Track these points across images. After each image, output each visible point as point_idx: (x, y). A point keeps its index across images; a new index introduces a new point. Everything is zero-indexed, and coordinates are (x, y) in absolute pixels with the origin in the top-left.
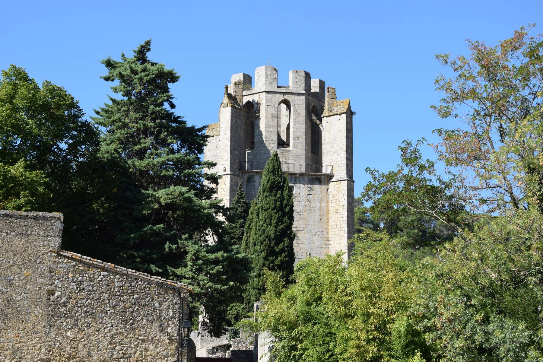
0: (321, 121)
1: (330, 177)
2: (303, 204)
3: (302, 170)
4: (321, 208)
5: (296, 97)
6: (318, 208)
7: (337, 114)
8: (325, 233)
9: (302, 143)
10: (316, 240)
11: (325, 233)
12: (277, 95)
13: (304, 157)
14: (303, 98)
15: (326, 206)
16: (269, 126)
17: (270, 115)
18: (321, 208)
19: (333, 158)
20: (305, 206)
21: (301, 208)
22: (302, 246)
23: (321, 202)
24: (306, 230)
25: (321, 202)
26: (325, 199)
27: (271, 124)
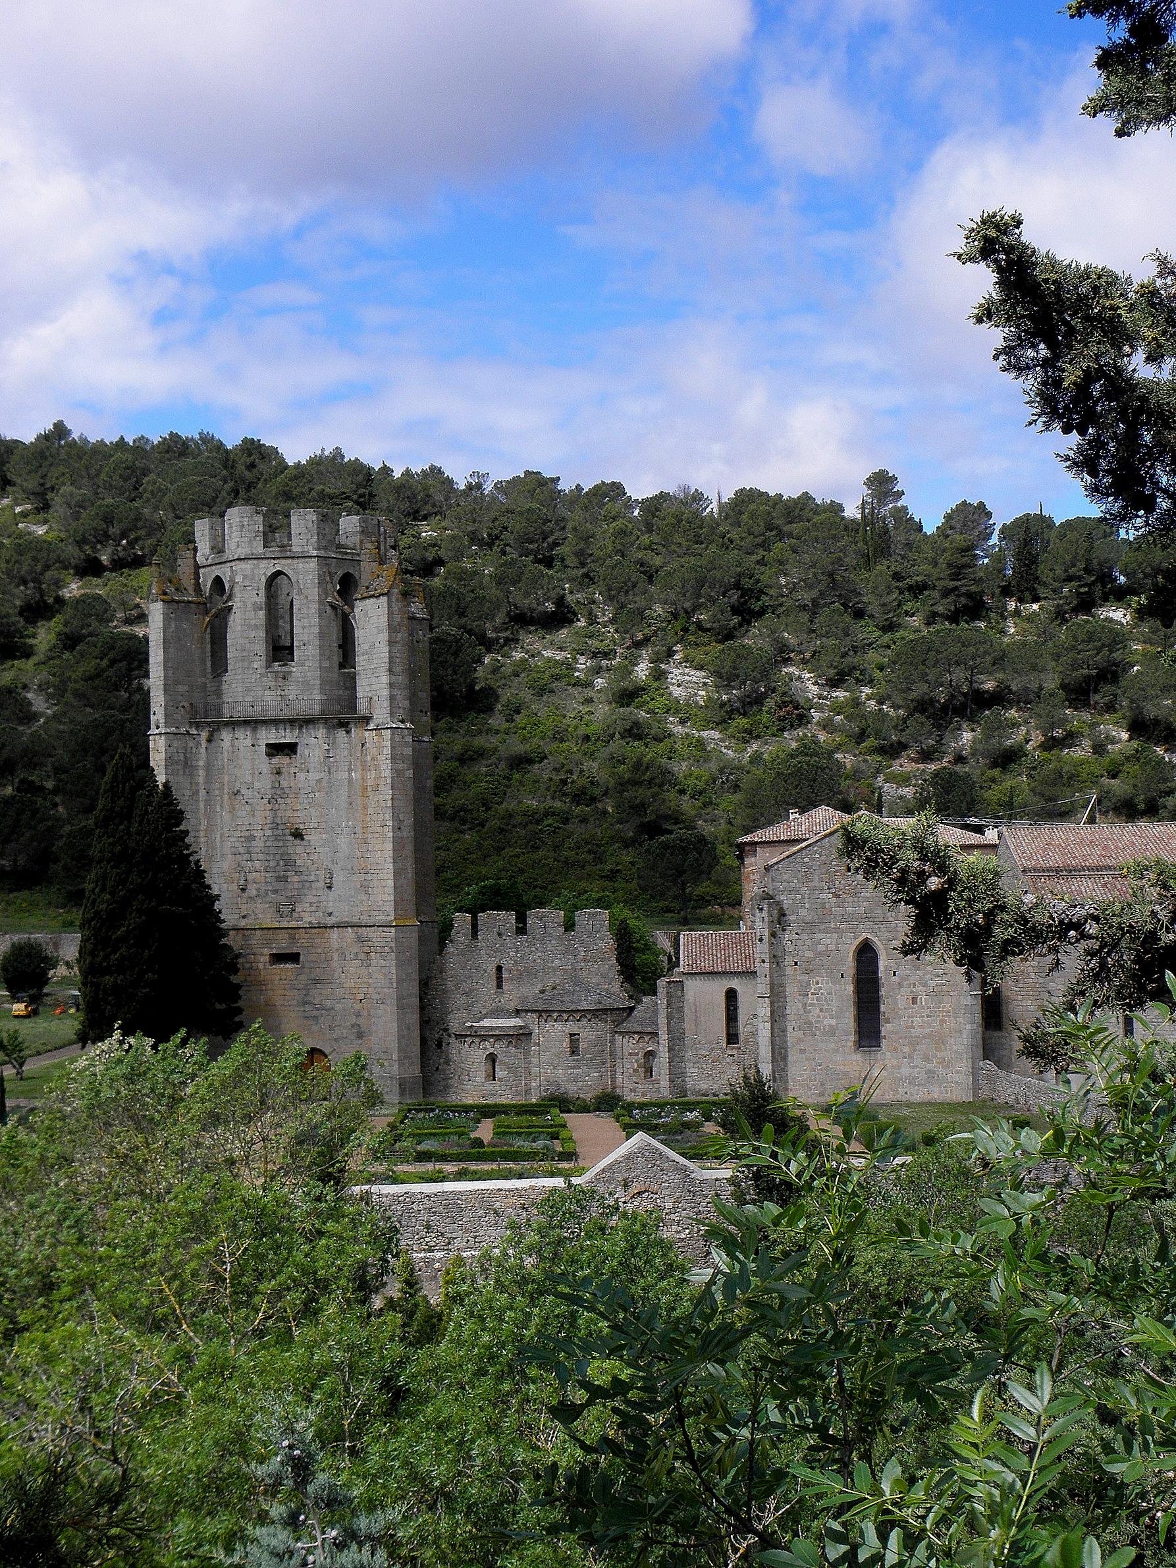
0: (353, 609)
1: (367, 719)
2: (317, 776)
3: (315, 710)
4: (350, 781)
5: (300, 564)
6: (346, 783)
7: (373, 596)
8: (359, 830)
9: (313, 656)
10: (343, 842)
11: (359, 830)
12: (263, 564)
13: (318, 682)
14: (313, 564)
15: (359, 777)
16: (249, 626)
17: (249, 605)
18: (350, 781)
19: (376, 681)
20: (319, 781)
21: (313, 783)
22: (315, 857)
23: (350, 770)
24: (323, 825)
25: (350, 770)
26: (358, 763)
27: (253, 622)
